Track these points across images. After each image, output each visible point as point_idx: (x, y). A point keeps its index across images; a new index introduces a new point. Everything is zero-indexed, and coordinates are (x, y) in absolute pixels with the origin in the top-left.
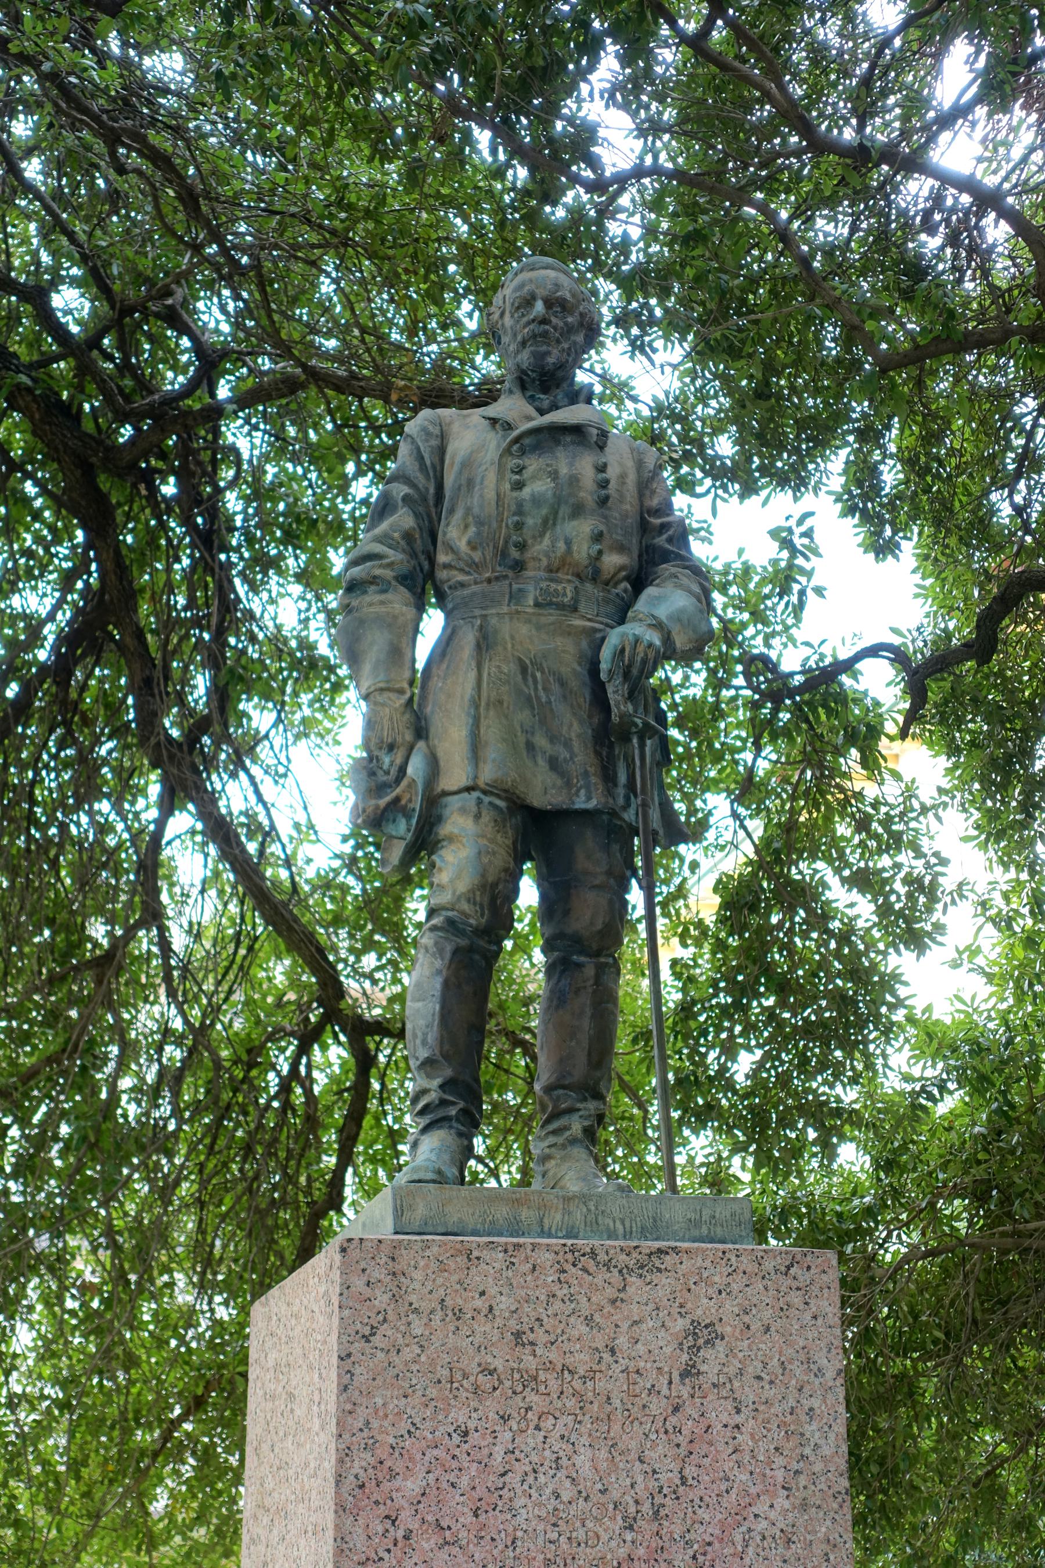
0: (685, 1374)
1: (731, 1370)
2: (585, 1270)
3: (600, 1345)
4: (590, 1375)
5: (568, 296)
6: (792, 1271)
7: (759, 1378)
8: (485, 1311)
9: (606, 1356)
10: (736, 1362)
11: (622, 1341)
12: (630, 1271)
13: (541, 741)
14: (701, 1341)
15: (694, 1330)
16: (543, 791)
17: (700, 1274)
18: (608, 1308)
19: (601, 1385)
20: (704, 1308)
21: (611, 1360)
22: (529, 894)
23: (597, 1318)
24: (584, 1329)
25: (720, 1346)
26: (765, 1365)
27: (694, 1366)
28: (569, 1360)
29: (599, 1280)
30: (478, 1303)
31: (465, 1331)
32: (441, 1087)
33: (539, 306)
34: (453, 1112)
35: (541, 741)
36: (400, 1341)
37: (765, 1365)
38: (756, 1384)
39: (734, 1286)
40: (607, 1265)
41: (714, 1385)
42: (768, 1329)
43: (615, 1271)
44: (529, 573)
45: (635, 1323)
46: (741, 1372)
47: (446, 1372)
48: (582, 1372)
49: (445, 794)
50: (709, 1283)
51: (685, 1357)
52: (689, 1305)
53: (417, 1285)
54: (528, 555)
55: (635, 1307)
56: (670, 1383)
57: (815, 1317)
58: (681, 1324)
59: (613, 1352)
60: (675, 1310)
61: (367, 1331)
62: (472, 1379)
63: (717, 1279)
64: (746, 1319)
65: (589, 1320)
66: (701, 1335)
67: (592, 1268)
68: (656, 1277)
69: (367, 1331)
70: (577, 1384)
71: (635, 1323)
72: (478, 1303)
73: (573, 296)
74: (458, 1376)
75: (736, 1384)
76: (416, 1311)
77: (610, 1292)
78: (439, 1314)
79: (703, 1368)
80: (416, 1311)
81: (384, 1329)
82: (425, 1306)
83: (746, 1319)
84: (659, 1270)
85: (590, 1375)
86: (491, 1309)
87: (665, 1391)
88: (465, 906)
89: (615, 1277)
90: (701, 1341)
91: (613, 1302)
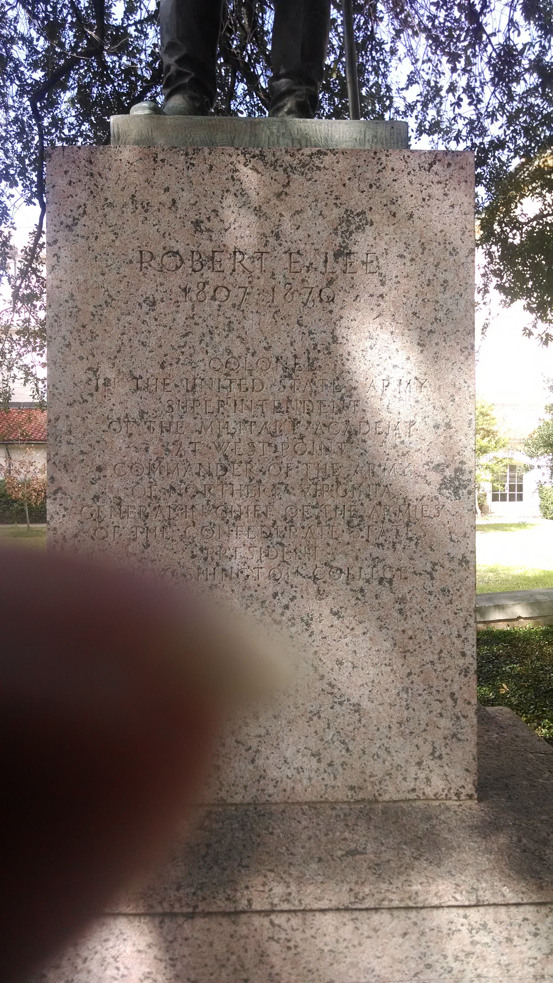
1: (379, 250)
3: (268, 232)
6: (435, 168)
7: (401, 256)
8: (169, 204)
9: (272, 240)
12: (293, 169)
14: (353, 227)
17: (354, 171)
18: (274, 201)
19: (268, 263)
21: (276, 243)
27: (346, 247)
30: (165, 198)
31: (152, 220)
32: (177, 62)
38: (400, 262)
41: (363, 263)
43: (281, 170)
45: (298, 212)
47: (137, 255)
51: (339, 240)
52: (344, 197)
53: (111, 184)
55: (297, 199)
56: (326, 261)
58: (336, 213)
59: (277, 236)
61: (70, 221)
62: (158, 259)
63: (368, 175)
68: (316, 175)
69: (70, 221)
71: (298, 212)
74: (147, 257)
75: (382, 261)
76: (111, 205)
79: (354, 249)
80: (111, 205)
81: (83, 220)
82: (119, 200)
83: (393, 208)
86: (174, 202)
87: (321, 268)
90: (353, 227)
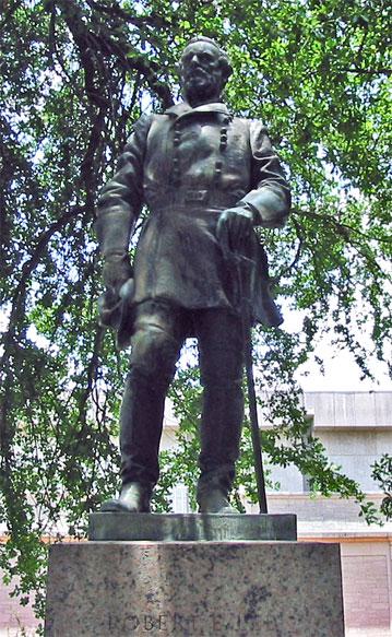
0: (248, 617)
1: (275, 613)
2: (189, 559)
3: (198, 601)
4: (193, 619)
5: (210, 53)
6: (312, 555)
7: (292, 618)
8: (130, 583)
9: (201, 608)
10: (278, 609)
11: (211, 599)
12: (216, 558)
13: (190, 273)
14: (258, 597)
15: (252, 593)
16: (189, 299)
17: (257, 559)
18: (202, 580)
19: (199, 624)
20: (259, 579)
21: (204, 610)
22: (189, 357)
23: (196, 586)
24: (188, 592)
25: (269, 600)
26: (296, 610)
27: (253, 612)
28: (179, 610)
29: (197, 565)
30: (126, 579)
31: (118, 595)
32: (132, 459)
33: (195, 58)
34: (138, 473)
35: (190, 273)
36: (82, 601)
37: (296, 610)
38: (291, 622)
39: (278, 565)
40: (202, 556)
41: (265, 623)
42: (297, 589)
43: (207, 559)
44: (182, 187)
45: (218, 588)
46: (281, 615)
47: (107, 619)
48: (186, 616)
49: (138, 304)
50: (262, 563)
51: (248, 607)
52: (250, 577)
53: (91, 570)
54: (182, 178)
55: (218, 580)
56: (239, 621)
57: (326, 582)
58: (245, 588)
59: (205, 605)
60: (242, 580)
61: (61, 596)
62: (122, 622)
63: (267, 561)
64: (285, 584)
65: (191, 587)
66: (257, 595)
67: (194, 558)
68: (232, 562)
69: (61, 596)
70: (183, 624)
71: (218, 588)
72: (126, 579)
73: (214, 53)
74: (114, 621)
75: (278, 621)
76: (91, 584)
77: (205, 571)
78: (104, 586)
79: (260, 613)
80: (91, 584)
81: (72, 594)
82: (96, 582)
83: (285, 584)
84: (233, 558)
85: (193, 619)
86: (134, 582)
87: (236, 627)
88: (144, 363)
89: (206, 562)
90: (258, 597)
91: (205, 576)
